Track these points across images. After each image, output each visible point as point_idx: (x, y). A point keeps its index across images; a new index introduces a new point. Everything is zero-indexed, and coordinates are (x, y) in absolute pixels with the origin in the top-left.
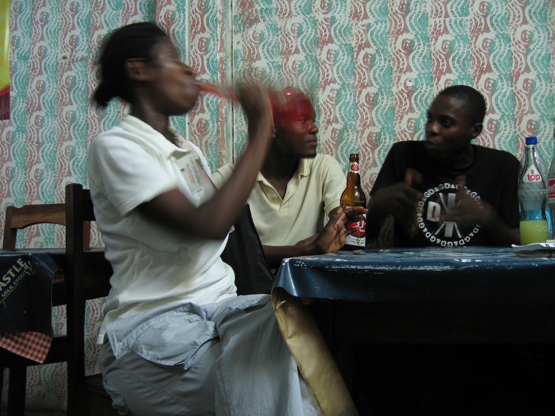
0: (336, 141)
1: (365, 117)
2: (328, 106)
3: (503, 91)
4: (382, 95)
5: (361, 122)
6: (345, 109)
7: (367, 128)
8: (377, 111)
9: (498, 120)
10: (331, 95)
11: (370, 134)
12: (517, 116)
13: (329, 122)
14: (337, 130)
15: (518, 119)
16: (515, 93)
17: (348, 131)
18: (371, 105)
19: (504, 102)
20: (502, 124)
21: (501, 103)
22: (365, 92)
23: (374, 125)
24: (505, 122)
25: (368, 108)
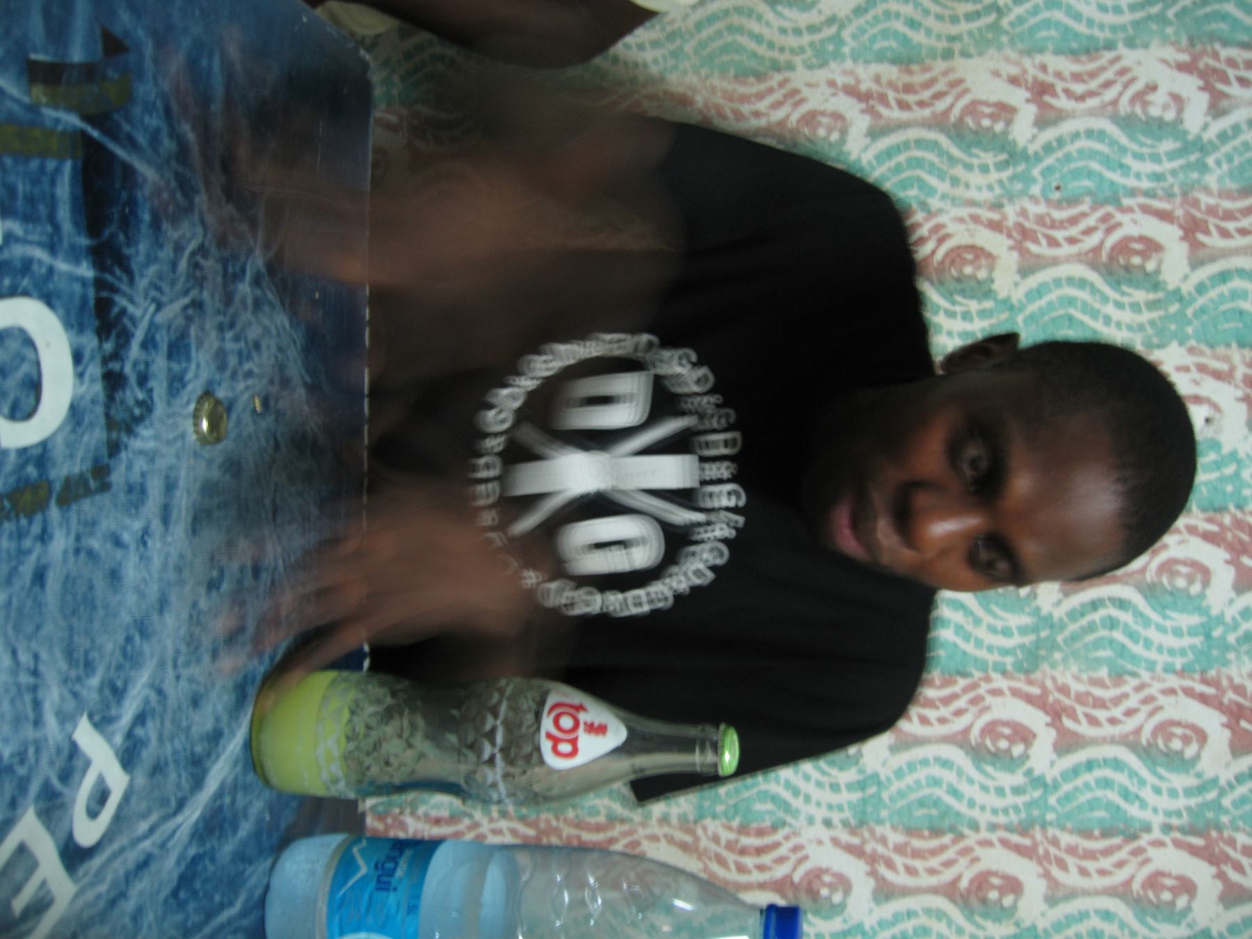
0: (961, 120)
1: (1059, 235)
2: (1108, 84)
3: (1147, 794)
4: (1152, 305)
5: (1040, 220)
6: (1092, 155)
7: (1011, 242)
8: (1082, 283)
9: (1028, 764)
10: (1159, 98)
11: (989, 256)
12: (1038, 836)
13: (1041, 91)
14: (1009, 122)
15: (1027, 842)
16: (1135, 837)
17: (1002, 166)
18: (1112, 258)
19: (1099, 793)
20: (1008, 780)
21: (1098, 781)
22: (1168, 234)
23: (1025, 271)
24: (1017, 790)
25: (1097, 250)
